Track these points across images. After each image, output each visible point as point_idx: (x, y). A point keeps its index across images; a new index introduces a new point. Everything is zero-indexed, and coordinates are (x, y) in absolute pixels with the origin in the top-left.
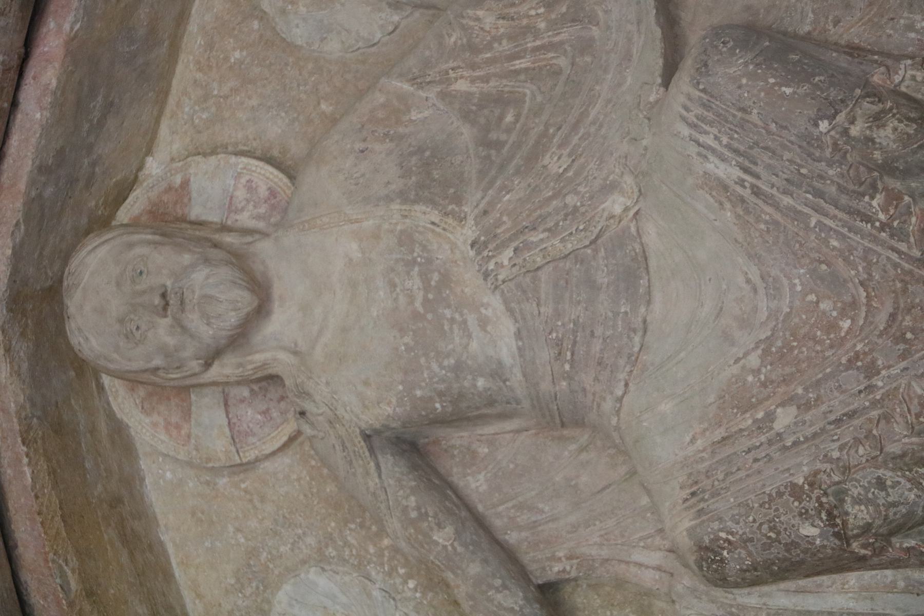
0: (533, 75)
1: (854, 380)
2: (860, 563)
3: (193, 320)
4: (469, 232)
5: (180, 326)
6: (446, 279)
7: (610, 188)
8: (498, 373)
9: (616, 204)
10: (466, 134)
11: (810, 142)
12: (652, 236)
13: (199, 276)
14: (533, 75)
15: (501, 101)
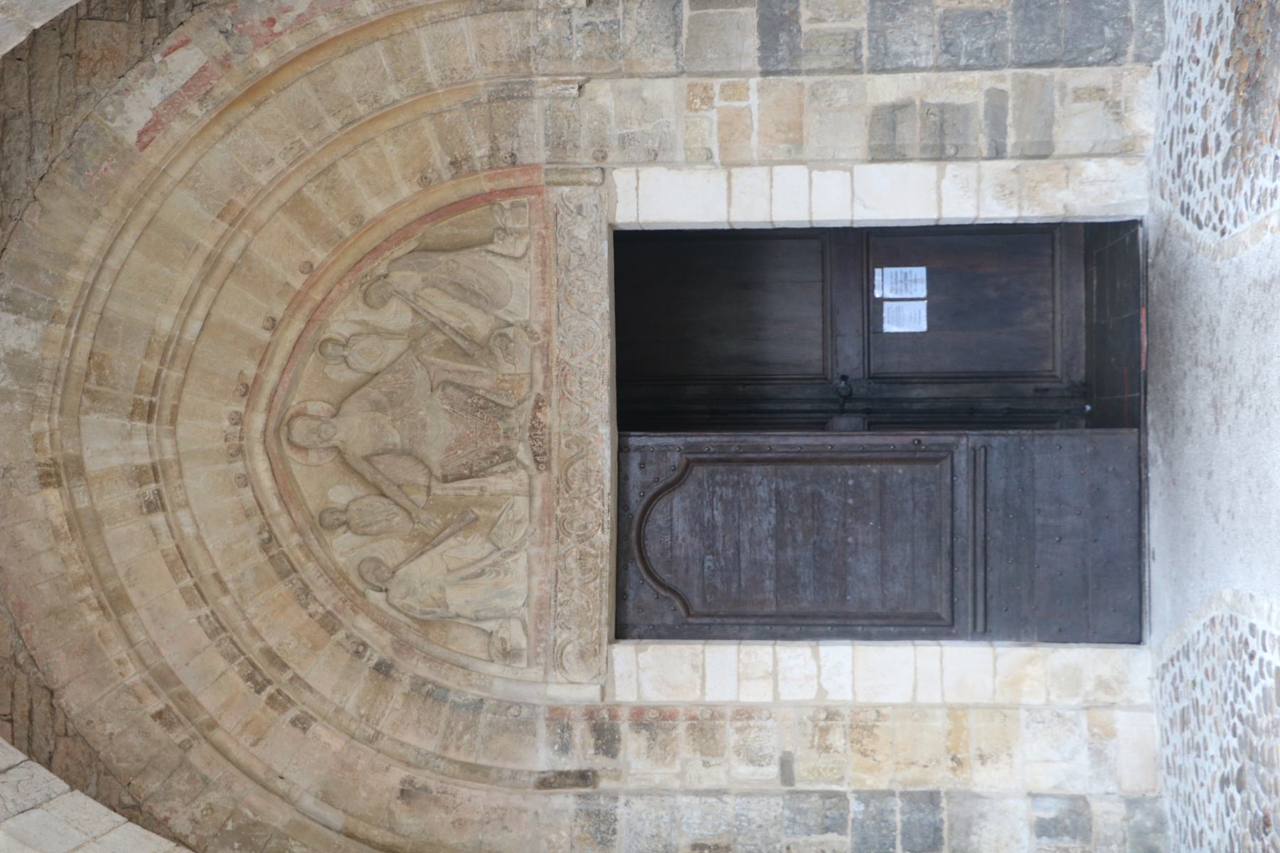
0: (400, 388)
1: (473, 445)
2: (473, 477)
3: (322, 435)
4: (390, 418)
5: (319, 436)
6: (383, 427)
7: (420, 410)
8: (395, 445)
9: (421, 413)
10: (385, 399)
11: (466, 403)
12: (428, 419)
13: (324, 426)
14: (400, 388)
15: (393, 393)
